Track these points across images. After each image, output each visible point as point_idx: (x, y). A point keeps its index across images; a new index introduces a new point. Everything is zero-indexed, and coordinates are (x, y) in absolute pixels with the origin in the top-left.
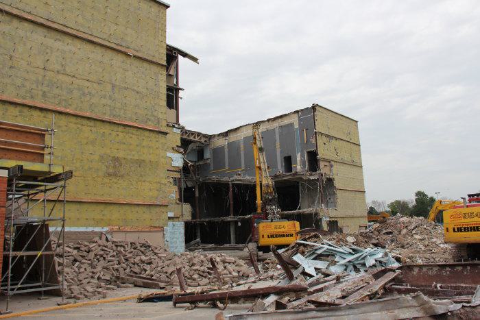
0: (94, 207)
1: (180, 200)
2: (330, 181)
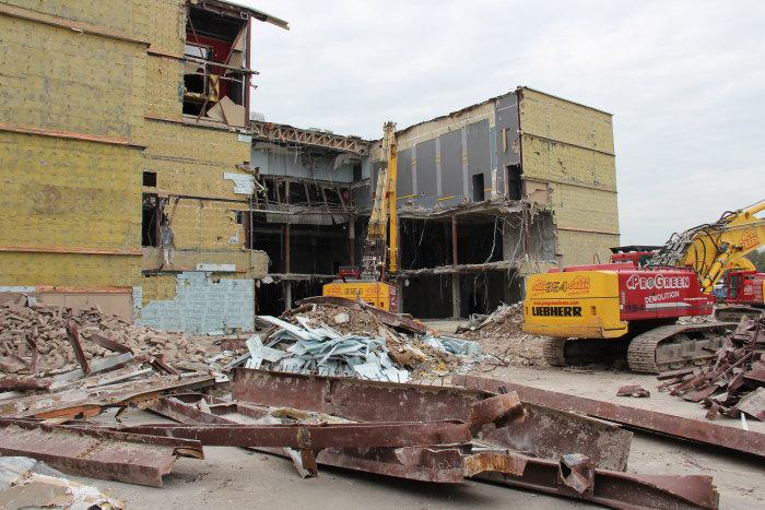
0: (13, 258)
1: (248, 245)
2: (546, 217)
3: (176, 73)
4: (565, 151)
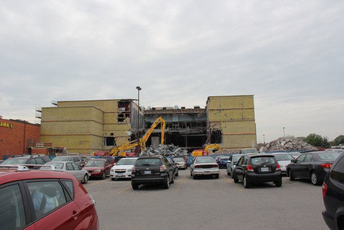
3: (117, 115)
4: (228, 111)
